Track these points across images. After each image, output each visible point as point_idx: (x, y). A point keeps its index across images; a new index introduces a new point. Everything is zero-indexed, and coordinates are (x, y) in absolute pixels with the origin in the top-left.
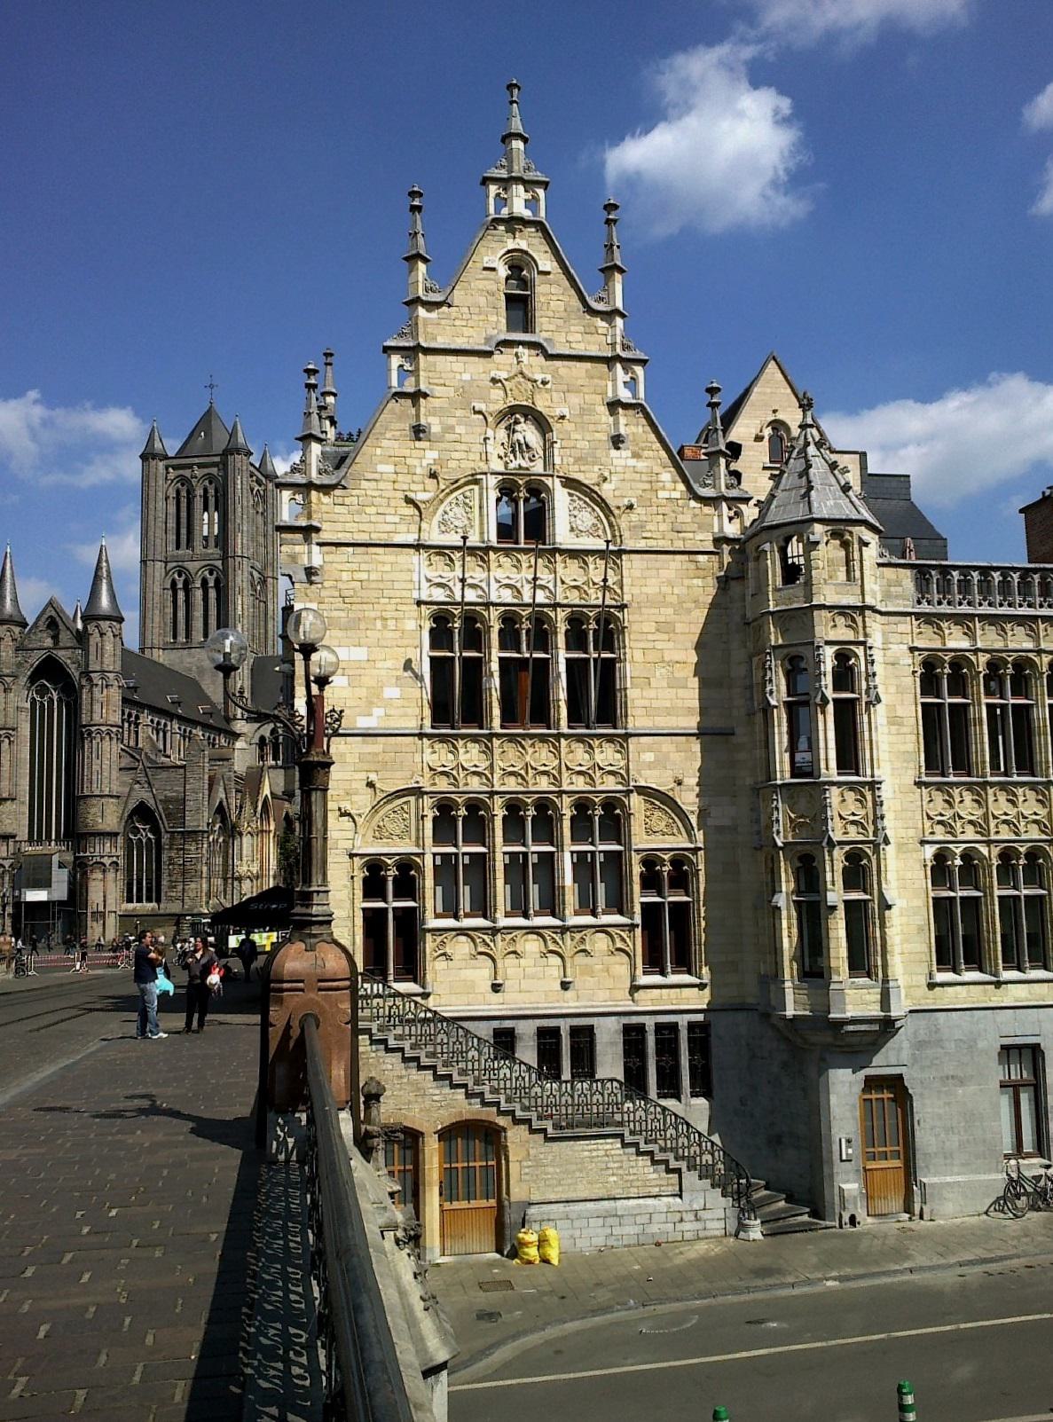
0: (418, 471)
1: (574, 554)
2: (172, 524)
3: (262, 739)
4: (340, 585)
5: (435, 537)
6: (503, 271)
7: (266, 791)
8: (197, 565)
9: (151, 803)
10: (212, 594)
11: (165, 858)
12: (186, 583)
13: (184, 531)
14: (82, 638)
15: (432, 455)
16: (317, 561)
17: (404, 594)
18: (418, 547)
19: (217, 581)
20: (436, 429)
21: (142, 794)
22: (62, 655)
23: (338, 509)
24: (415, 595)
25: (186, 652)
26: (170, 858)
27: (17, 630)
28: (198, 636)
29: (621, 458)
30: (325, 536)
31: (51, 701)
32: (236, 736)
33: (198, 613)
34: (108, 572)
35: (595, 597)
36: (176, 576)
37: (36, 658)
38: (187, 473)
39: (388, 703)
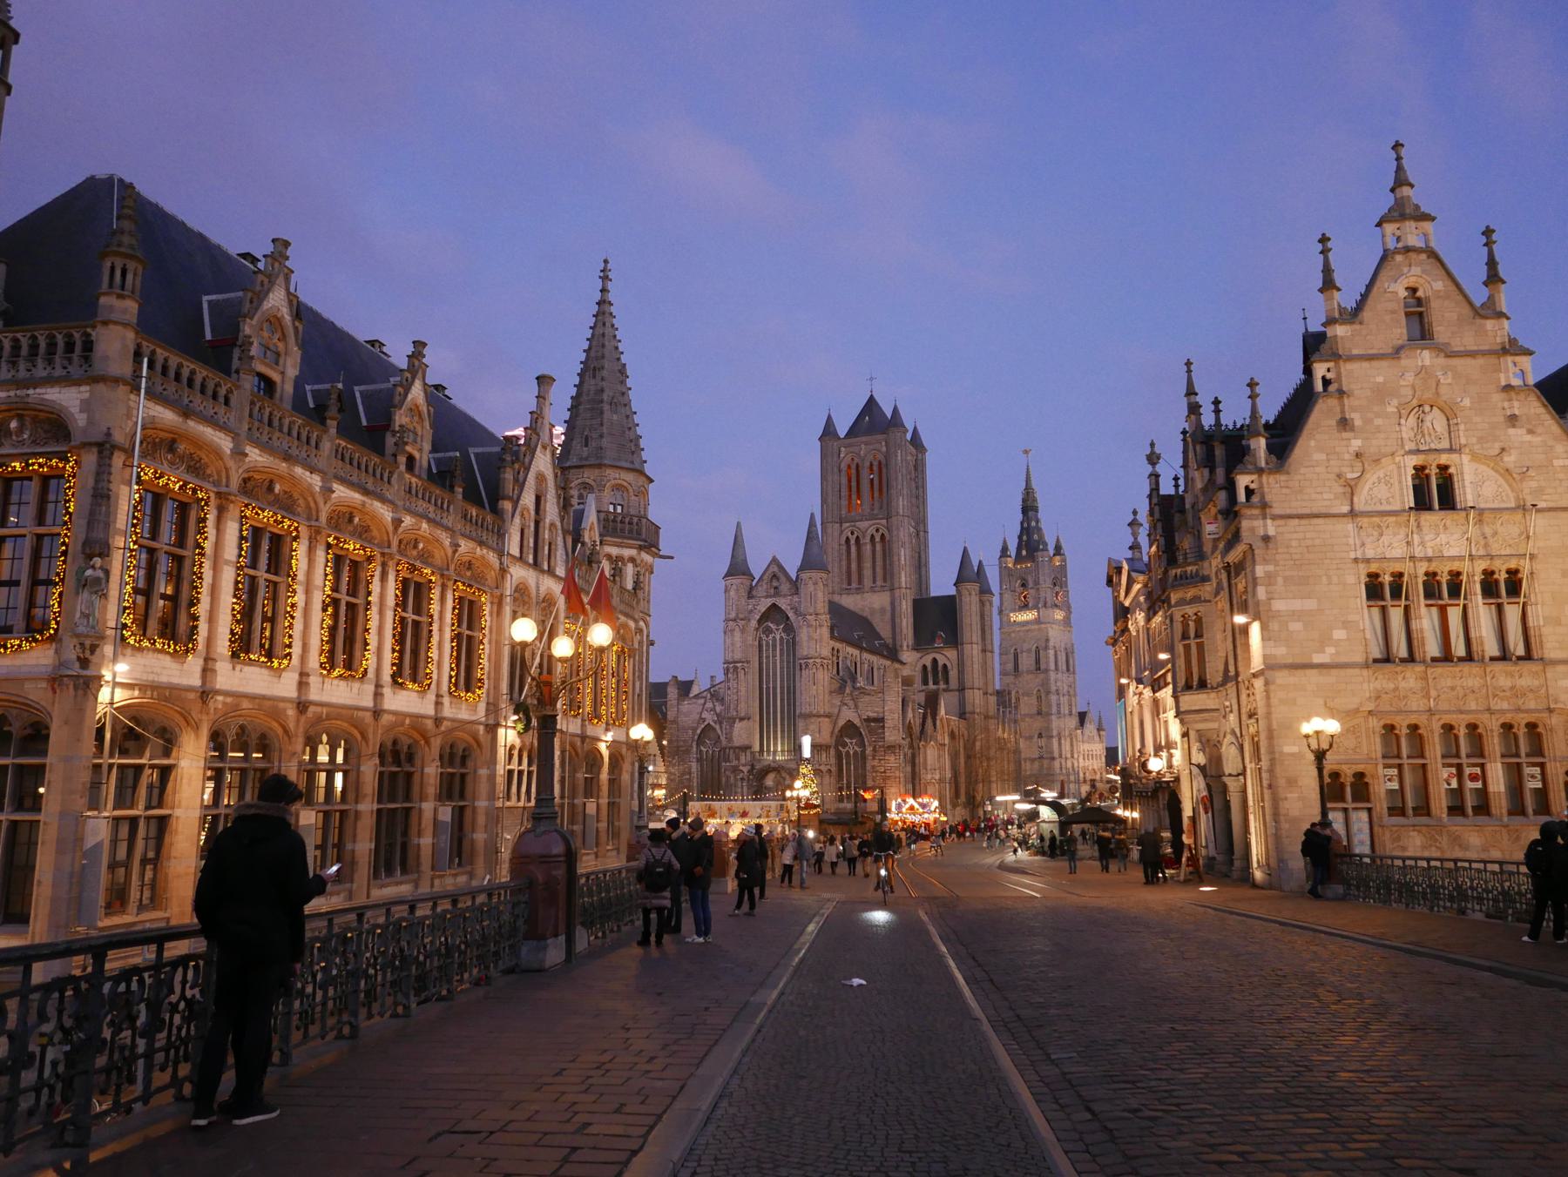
0: (1347, 456)
2: (845, 493)
3: (925, 667)
4: (1292, 550)
6: (1403, 293)
7: (942, 712)
9: (857, 722)
10: (878, 547)
11: (868, 767)
14: (795, 586)
15: (1356, 444)
16: (1271, 532)
17: (1344, 555)
18: (1353, 514)
20: (1358, 423)
21: (848, 714)
22: (783, 603)
23: (1284, 491)
24: (1353, 555)
25: (859, 597)
26: (873, 767)
28: (867, 582)
29: (1517, 434)
30: (1277, 511)
33: (867, 565)
37: (764, 605)
38: (856, 449)
39: (1337, 643)
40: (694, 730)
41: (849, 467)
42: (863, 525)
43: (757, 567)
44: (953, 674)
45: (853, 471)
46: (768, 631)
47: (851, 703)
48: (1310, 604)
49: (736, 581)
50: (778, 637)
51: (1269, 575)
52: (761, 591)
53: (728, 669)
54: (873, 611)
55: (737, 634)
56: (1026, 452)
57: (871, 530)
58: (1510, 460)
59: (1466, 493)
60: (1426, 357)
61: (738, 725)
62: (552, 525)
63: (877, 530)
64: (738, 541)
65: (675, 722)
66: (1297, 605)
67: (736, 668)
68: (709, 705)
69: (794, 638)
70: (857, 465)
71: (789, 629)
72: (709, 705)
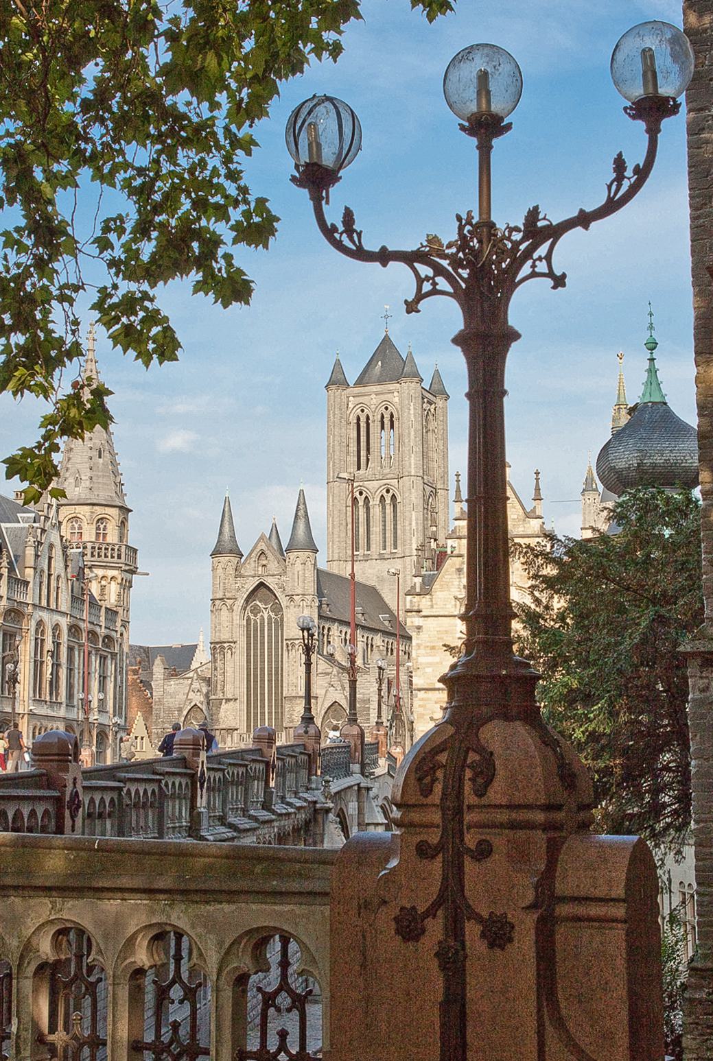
2: (353, 448)
8: (376, 484)
10: (389, 509)
13: (363, 453)
22: (271, 582)
27: (235, 560)
31: (262, 618)
34: (306, 512)
36: (358, 493)
37: (251, 584)
40: (180, 710)
41: (358, 419)
42: (373, 485)
45: (363, 424)
46: (255, 611)
47: (336, 683)
49: (224, 559)
50: (266, 616)
51: (419, 646)
52: (248, 569)
53: (215, 648)
54: (381, 580)
61: (224, 706)
62: (59, 577)
63: (388, 491)
64: (226, 516)
65: (160, 702)
66: (430, 659)
67: (224, 648)
68: (196, 685)
69: (282, 620)
70: (368, 418)
71: (278, 609)
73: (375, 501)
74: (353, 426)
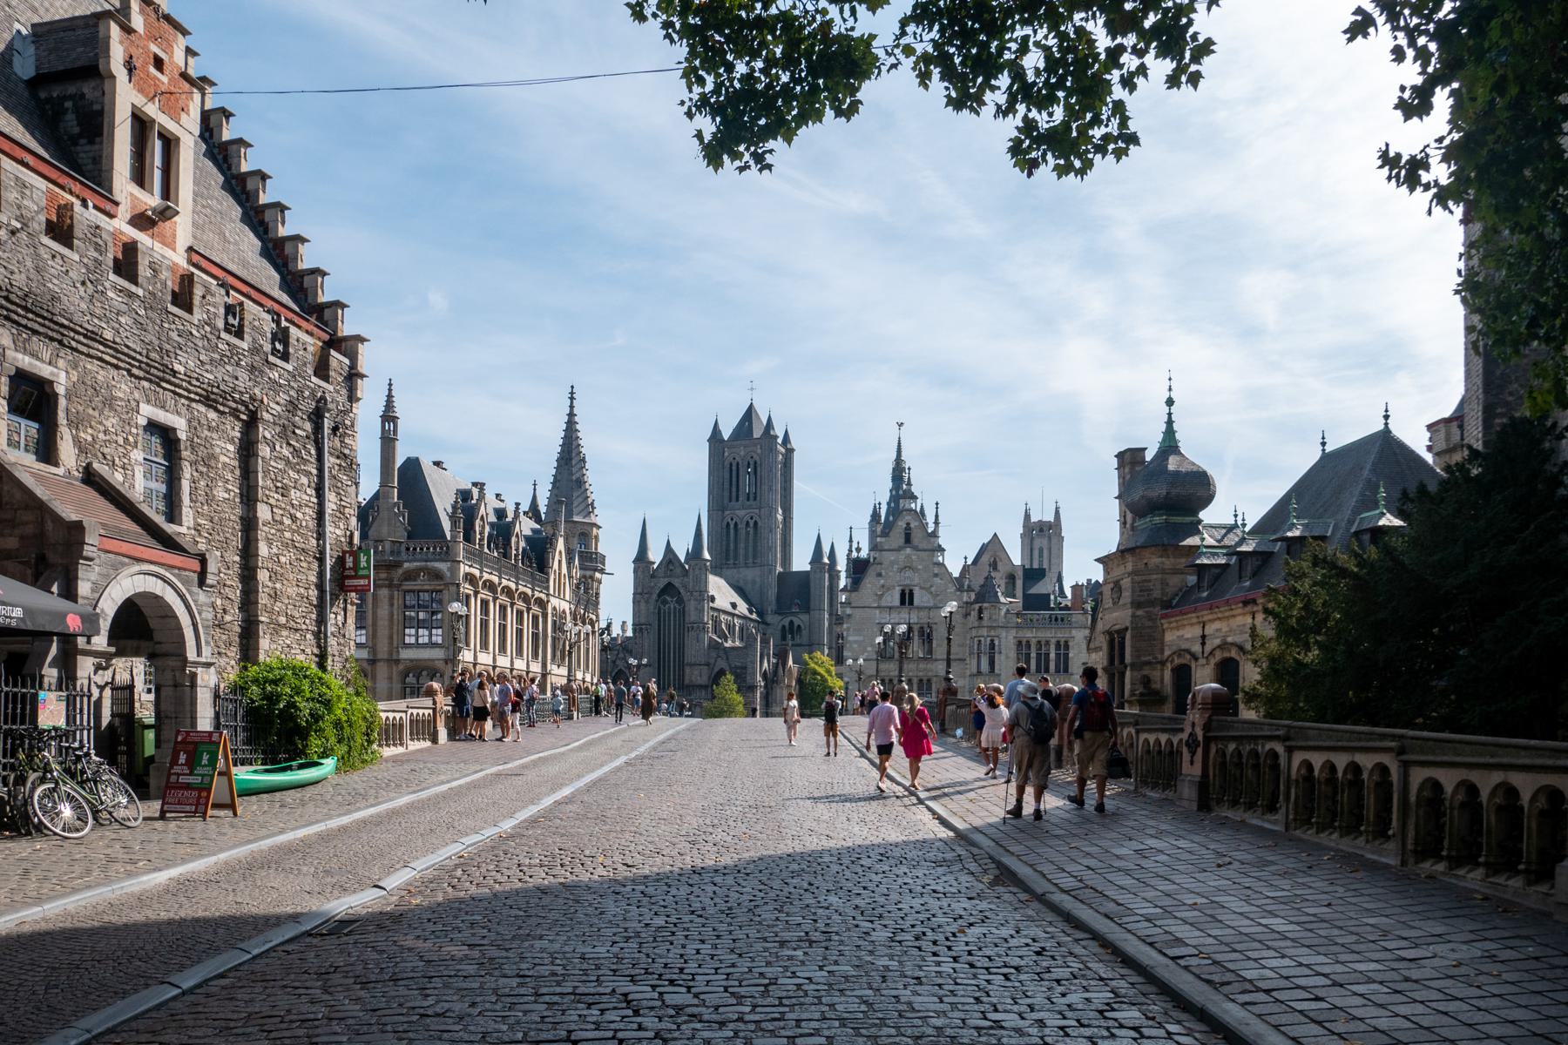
1: (920, 608)
2: (727, 485)
3: (784, 627)
5: (883, 604)
12: (736, 524)
13: (734, 489)
19: (756, 523)
22: (677, 582)
29: (937, 580)
32: (767, 624)
35: (926, 620)
37: (662, 583)
42: (741, 513)
43: (656, 555)
44: (805, 633)
45: (734, 468)
46: (665, 602)
48: (861, 638)
55: (643, 605)
56: (901, 425)
57: (747, 518)
58: (933, 589)
59: (916, 602)
60: (908, 550)
66: (856, 638)
71: (680, 601)
72: (621, 655)
73: (741, 526)
74: (727, 469)
